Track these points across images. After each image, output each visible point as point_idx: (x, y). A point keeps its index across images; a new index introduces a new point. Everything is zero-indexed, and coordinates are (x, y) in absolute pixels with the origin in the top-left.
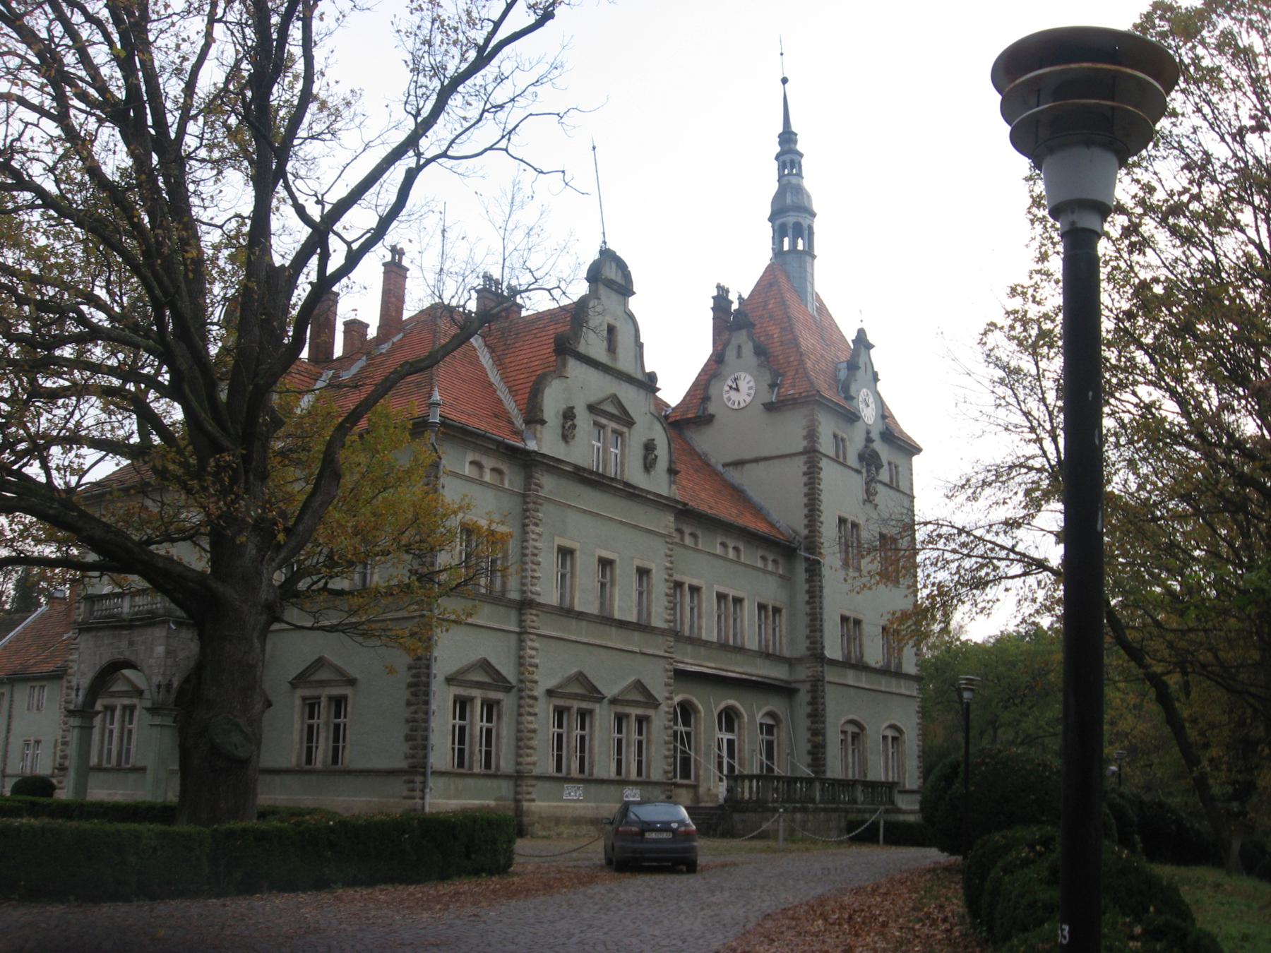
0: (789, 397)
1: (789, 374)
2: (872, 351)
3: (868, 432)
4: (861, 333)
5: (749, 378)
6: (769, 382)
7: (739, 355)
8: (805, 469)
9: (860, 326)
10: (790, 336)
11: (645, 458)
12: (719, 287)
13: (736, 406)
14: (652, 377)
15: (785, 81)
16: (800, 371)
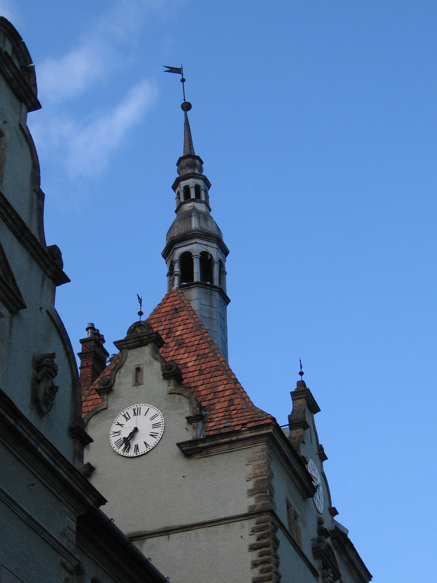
0: (223, 431)
1: (218, 406)
2: (316, 416)
3: (320, 522)
4: (301, 384)
5: (153, 411)
6: (188, 415)
7: (137, 382)
8: (253, 540)
9: (299, 378)
10: (214, 363)
11: (36, 382)
12: (91, 328)
13: (132, 453)
14: (55, 251)
15: (186, 107)
16: (237, 401)
